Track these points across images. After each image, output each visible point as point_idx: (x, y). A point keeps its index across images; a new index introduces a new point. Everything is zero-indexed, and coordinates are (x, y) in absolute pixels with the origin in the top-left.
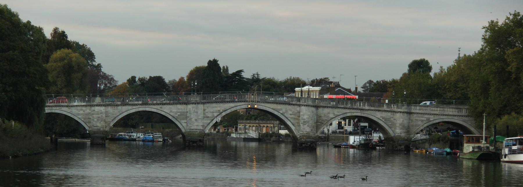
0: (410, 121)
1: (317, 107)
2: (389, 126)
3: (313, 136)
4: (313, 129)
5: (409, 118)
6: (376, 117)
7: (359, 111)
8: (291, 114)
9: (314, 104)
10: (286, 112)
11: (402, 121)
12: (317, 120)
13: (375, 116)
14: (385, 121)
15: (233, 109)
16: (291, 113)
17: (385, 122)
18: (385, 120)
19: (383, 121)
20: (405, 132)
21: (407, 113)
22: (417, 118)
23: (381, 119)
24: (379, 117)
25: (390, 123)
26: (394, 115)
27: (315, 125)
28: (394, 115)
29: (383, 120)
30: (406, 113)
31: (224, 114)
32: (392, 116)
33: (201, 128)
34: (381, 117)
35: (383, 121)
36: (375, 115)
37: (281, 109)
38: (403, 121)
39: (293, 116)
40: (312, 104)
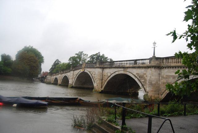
0: (161, 77)
1: (103, 68)
2: (142, 83)
3: (98, 90)
4: (98, 85)
5: (159, 74)
6: (133, 74)
7: (123, 69)
8: (94, 75)
9: (100, 66)
10: (93, 73)
11: (149, 77)
12: (102, 78)
13: (132, 73)
14: (139, 78)
15: (80, 73)
16: (94, 74)
17: (139, 79)
18: (140, 77)
19: (138, 79)
20: (152, 91)
21: (155, 67)
22: (167, 74)
23: (136, 75)
24: (135, 74)
25: (143, 81)
26: (146, 71)
27: (101, 82)
28: (146, 71)
29: (138, 77)
30: (153, 68)
31: (77, 76)
32: (145, 72)
33: (72, 83)
34: (137, 74)
35: (138, 79)
36: (132, 72)
37: (91, 72)
38: (150, 77)
39: (94, 76)
40: (98, 66)
